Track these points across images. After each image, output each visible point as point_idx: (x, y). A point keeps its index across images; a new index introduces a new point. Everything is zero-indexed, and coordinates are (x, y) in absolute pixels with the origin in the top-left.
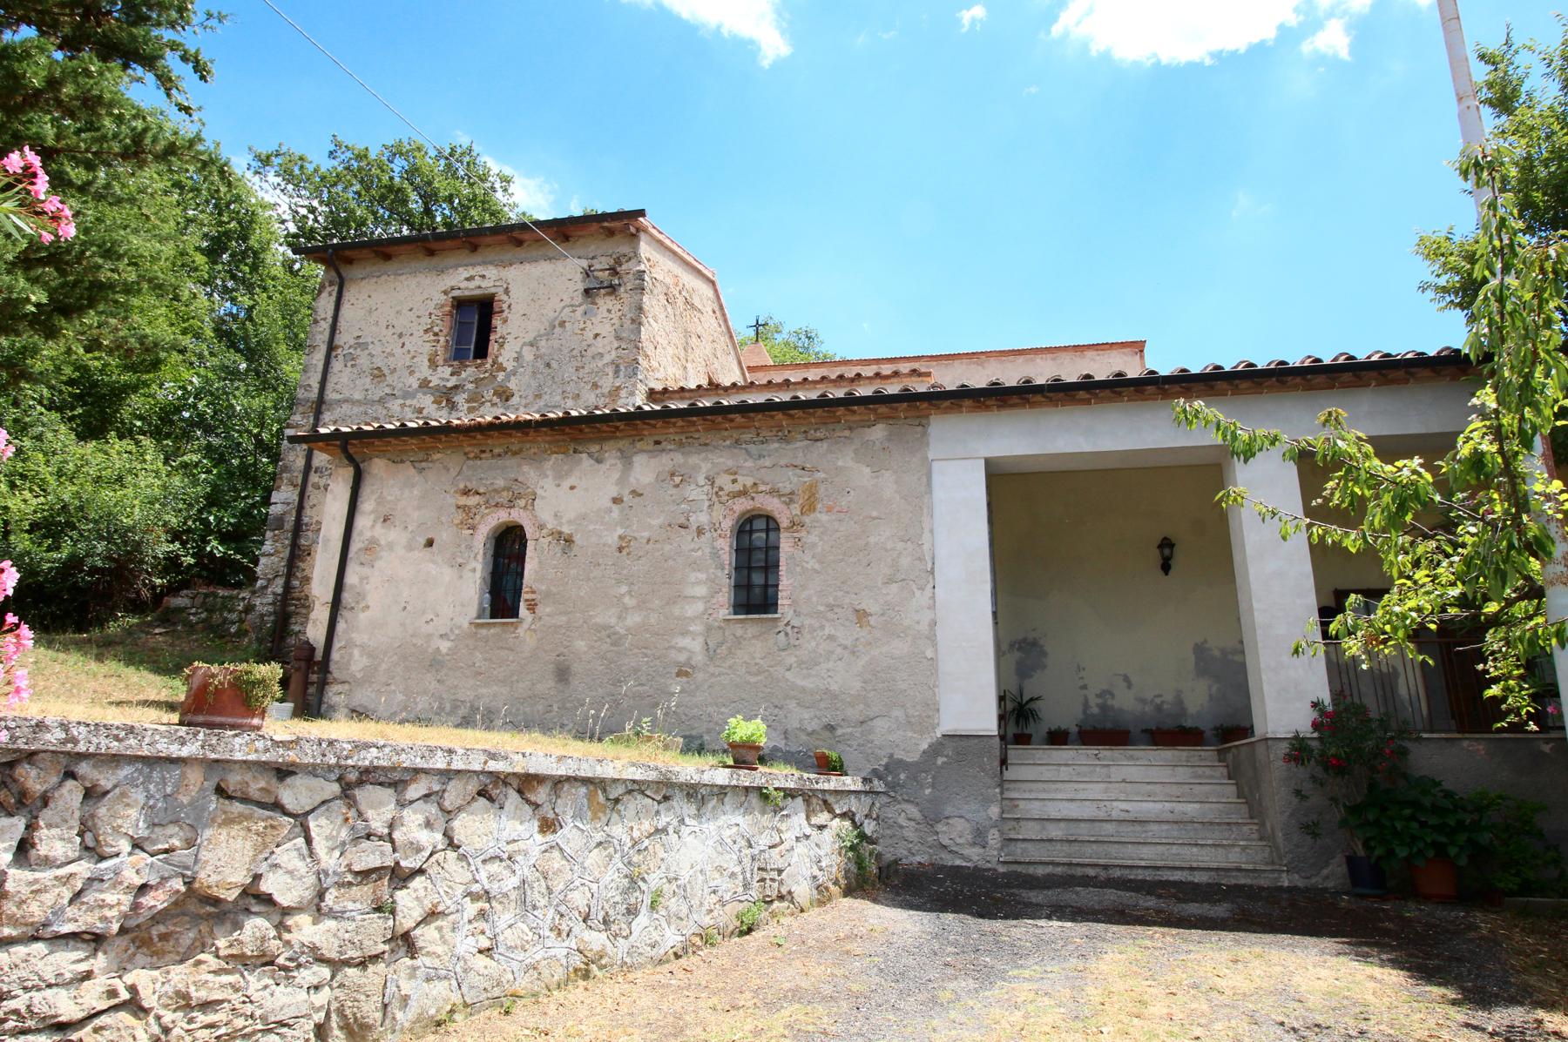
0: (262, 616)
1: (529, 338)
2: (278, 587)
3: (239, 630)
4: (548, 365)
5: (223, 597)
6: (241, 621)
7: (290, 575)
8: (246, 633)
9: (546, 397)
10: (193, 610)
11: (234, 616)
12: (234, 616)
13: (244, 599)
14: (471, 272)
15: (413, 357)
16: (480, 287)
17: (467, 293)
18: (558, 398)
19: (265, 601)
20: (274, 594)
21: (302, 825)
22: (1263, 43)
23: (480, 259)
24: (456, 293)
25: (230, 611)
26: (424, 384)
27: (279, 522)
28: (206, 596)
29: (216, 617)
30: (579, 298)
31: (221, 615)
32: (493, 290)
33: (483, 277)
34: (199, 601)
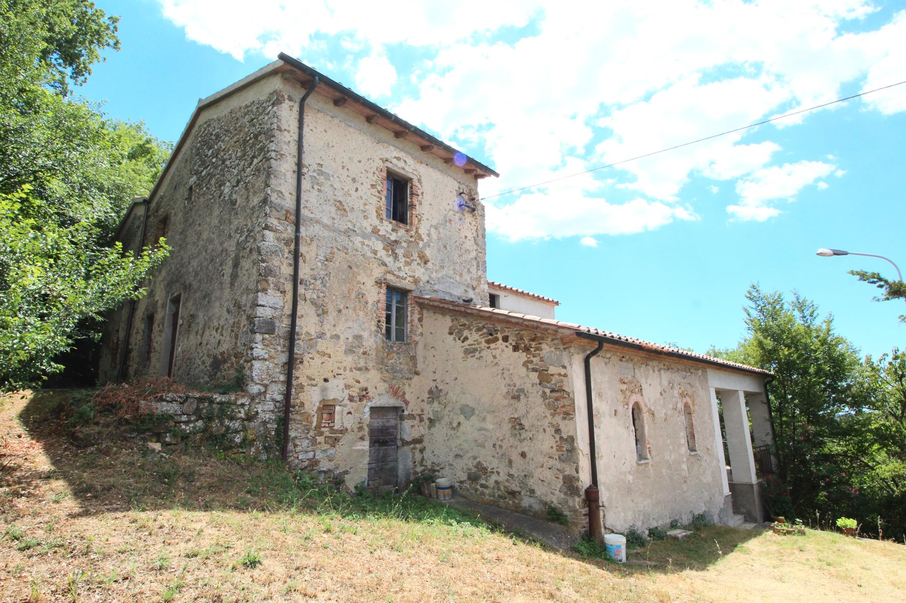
0: (264, 423)
1: (434, 222)
2: (276, 392)
3: (244, 440)
4: (445, 247)
5: (221, 403)
6: (245, 429)
7: (289, 383)
8: (251, 443)
9: (446, 269)
10: (184, 418)
11: (236, 425)
12: (236, 425)
13: (243, 405)
14: (402, 155)
15: (365, 204)
16: (404, 169)
17: (396, 169)
18: (452, 272)
19: (266, 408)
20: (273, 400)
21: (554, 515)
22: (607, 201)
23: (401, 146)
24: (390, 165)
25: (232, 418)
26: (375, 231)
27: (269, 327)
28: (201, 400)
29: (215, 425)
30: (457, 208)
31: (222, 424)
32: (411, 176)
33: (405, 162)
34: (190, 407)
